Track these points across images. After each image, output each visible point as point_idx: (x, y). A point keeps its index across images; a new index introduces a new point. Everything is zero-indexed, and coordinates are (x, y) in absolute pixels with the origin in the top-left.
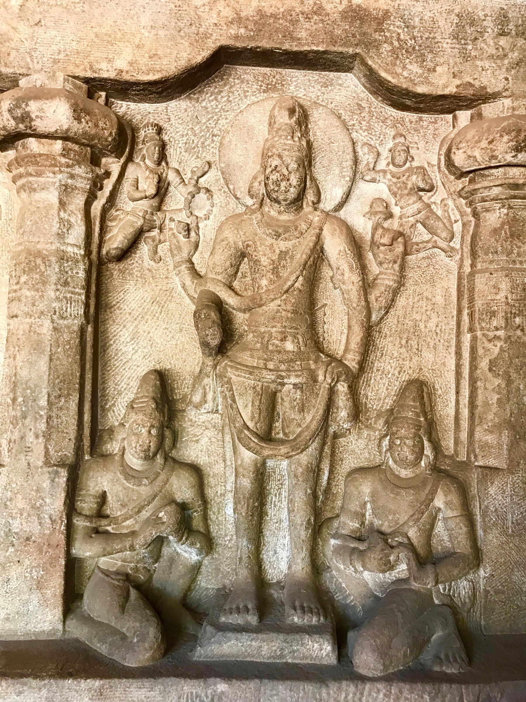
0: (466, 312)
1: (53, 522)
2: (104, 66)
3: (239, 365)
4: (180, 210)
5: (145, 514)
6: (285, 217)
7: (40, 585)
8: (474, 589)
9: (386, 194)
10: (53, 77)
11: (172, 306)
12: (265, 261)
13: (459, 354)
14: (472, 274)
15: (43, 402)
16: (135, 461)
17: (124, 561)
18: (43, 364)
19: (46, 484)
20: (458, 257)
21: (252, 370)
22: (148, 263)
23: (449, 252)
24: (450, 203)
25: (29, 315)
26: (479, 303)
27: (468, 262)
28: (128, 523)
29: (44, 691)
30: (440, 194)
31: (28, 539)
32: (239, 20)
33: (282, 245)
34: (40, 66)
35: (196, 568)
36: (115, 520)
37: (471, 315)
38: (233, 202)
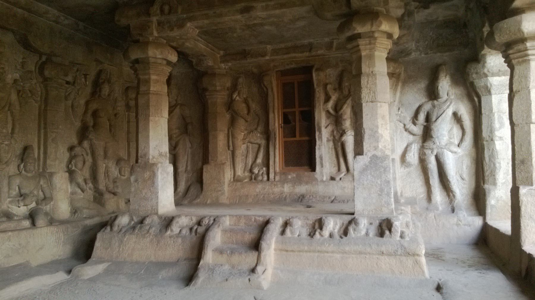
0: (42, 122)
9: (18, 78)
13: (39, 137)
14: (45, 110)
23: (36, 102)
24: (38, 85)
27: (43, 107)
30: (34, 81)
37: (45, 124)
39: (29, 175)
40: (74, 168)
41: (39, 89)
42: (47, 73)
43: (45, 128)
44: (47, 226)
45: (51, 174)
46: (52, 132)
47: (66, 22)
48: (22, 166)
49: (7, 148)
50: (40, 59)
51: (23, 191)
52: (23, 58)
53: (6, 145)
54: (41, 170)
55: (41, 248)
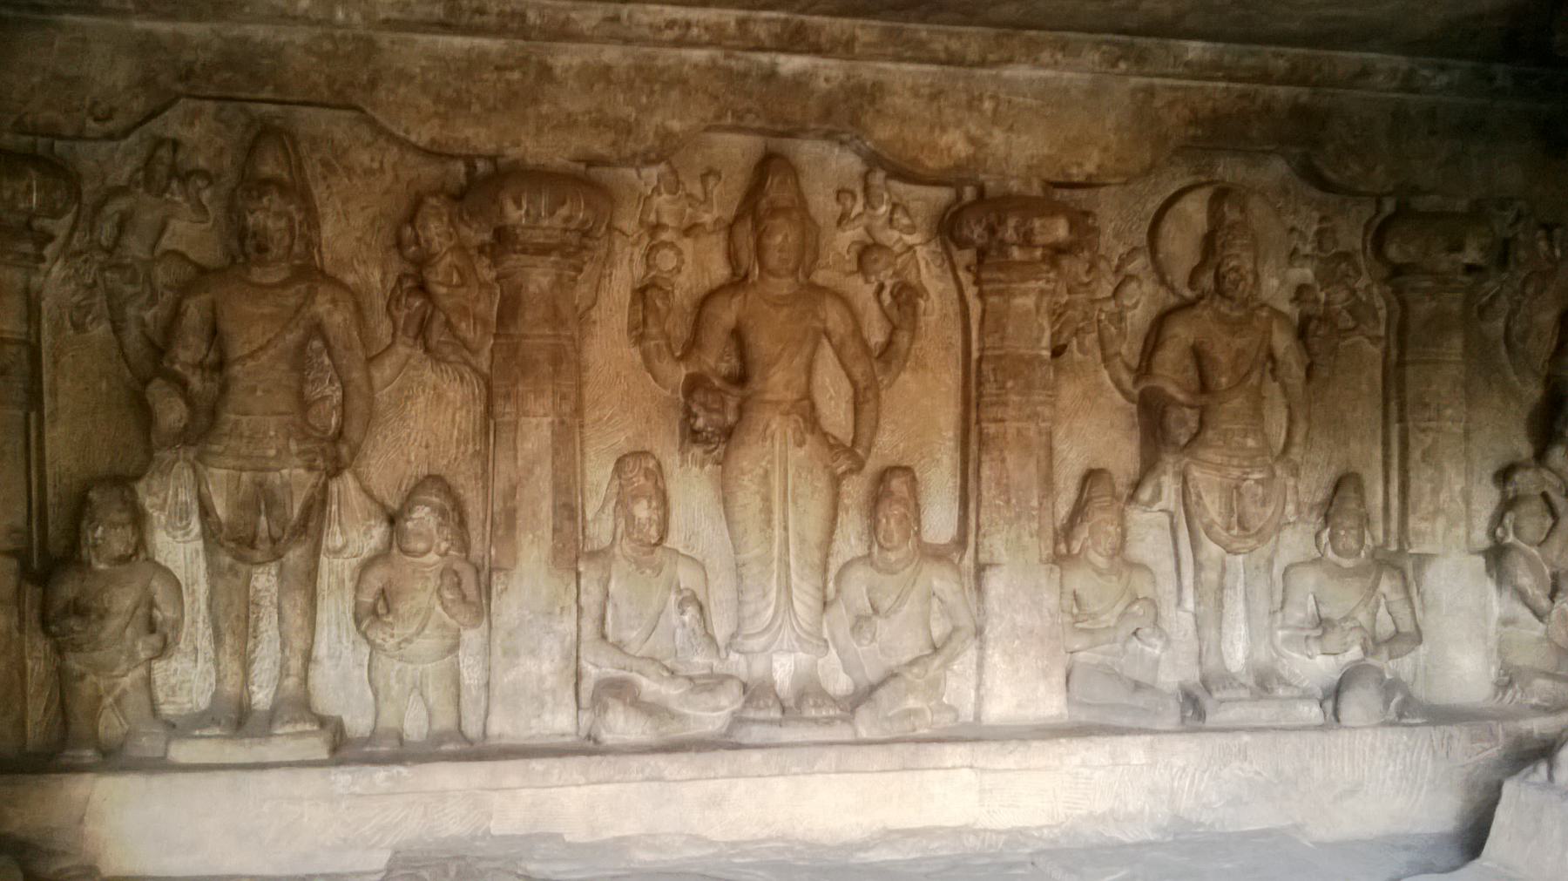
1: (1052, 616)
2: (1074, 170)
3: (1203, 463)
4: (1107, 299)
5: (1119, 608)
6: (1236, 314)
7: (1045, 674)
8: (1416, 666)
10: (1028, 183)
11: (1102, 400)
12: (1223, 359)
13: (1386, 444)
14: (1401, 364)
15: (1035, 503)
16: (1101, 562)
17: (1104, 653)
18: (1032, 467)
19: (1043, 581)
20: (1383, 344)
21: (1219, 468)
22: (1078, 356)
23: (1374, 340)
24: (1375, 290)
25: (1019, 420)
26: (1410, 395)
27: (1394, 353)
28: (1104, 618)
29: (1107, 748)
31: (1031, 632)
32: (1195, 121)
33: (1239, 343)
34: (1014, 173)
35: (1157, 662)
36: (1094, 616)
38: (1162, 292)
39: (1347, 563)
40: (1511, 539)
41: (1379, 302)
42: (1393, 252)
43: (1402, 420)
44: (1375, 727)
45: (1422, 560)
46: (1423, 430)
47: (1443, 79)
48: (1325, 535)
49: (1260, 490)
50: (1378, 212)
51: (1325, 611)
52: (1322, 219)
53: (1257, 481)
54: (1394, 547)
55: (1353, 792)
